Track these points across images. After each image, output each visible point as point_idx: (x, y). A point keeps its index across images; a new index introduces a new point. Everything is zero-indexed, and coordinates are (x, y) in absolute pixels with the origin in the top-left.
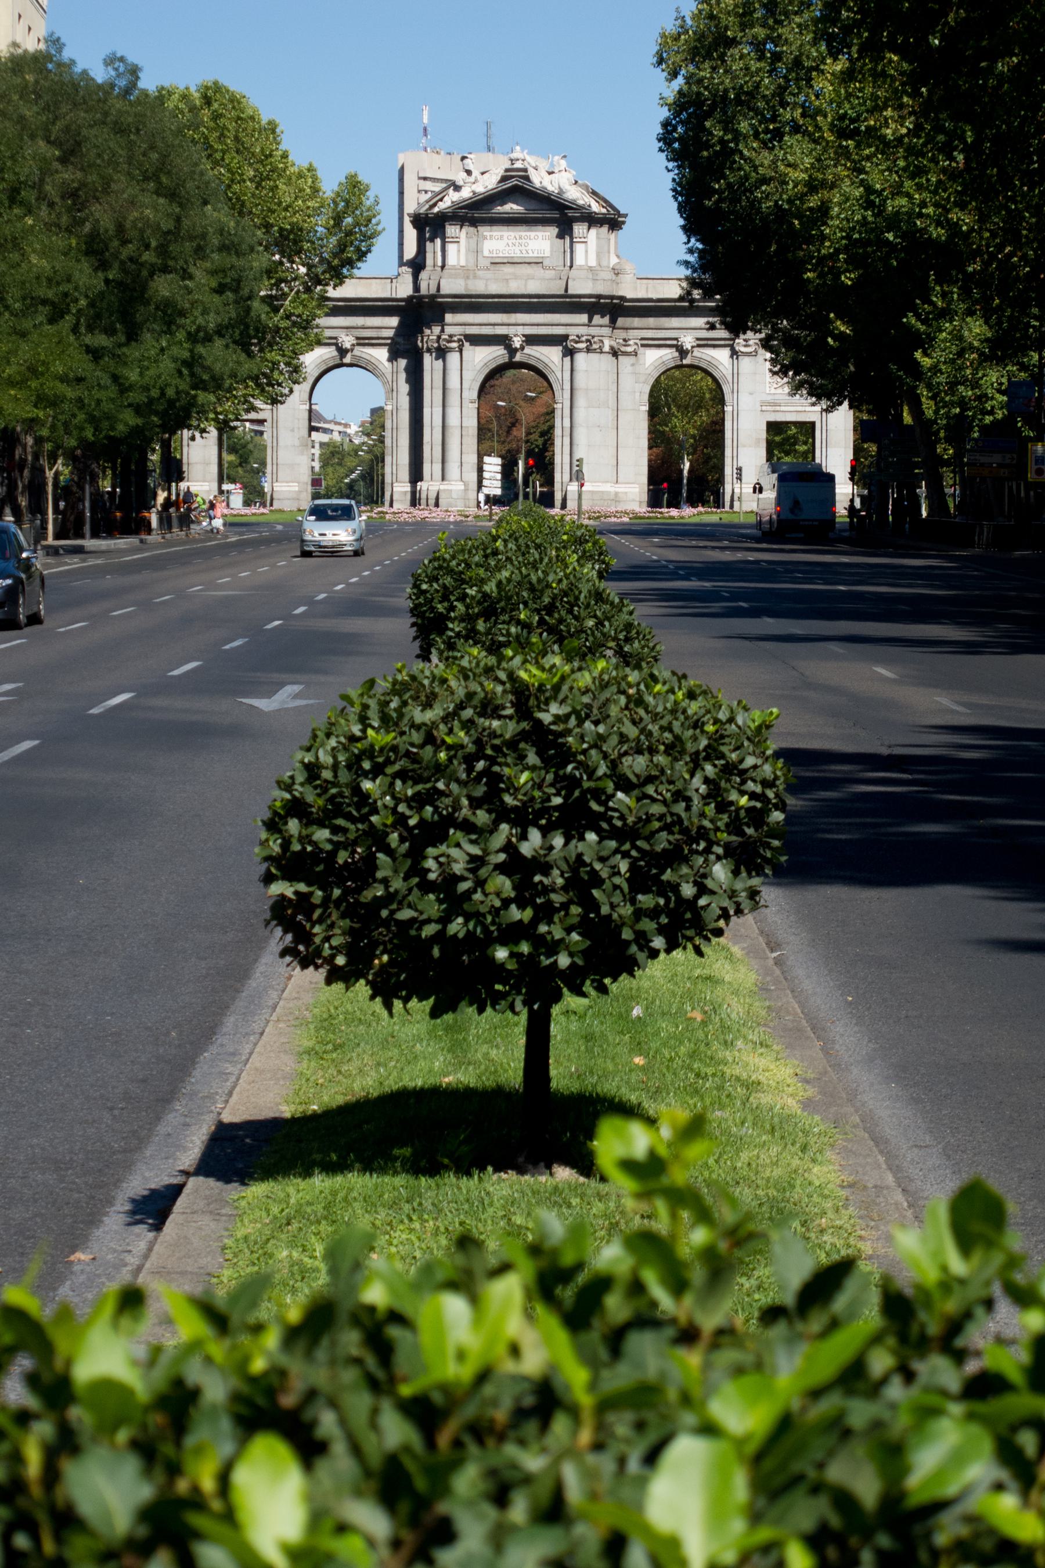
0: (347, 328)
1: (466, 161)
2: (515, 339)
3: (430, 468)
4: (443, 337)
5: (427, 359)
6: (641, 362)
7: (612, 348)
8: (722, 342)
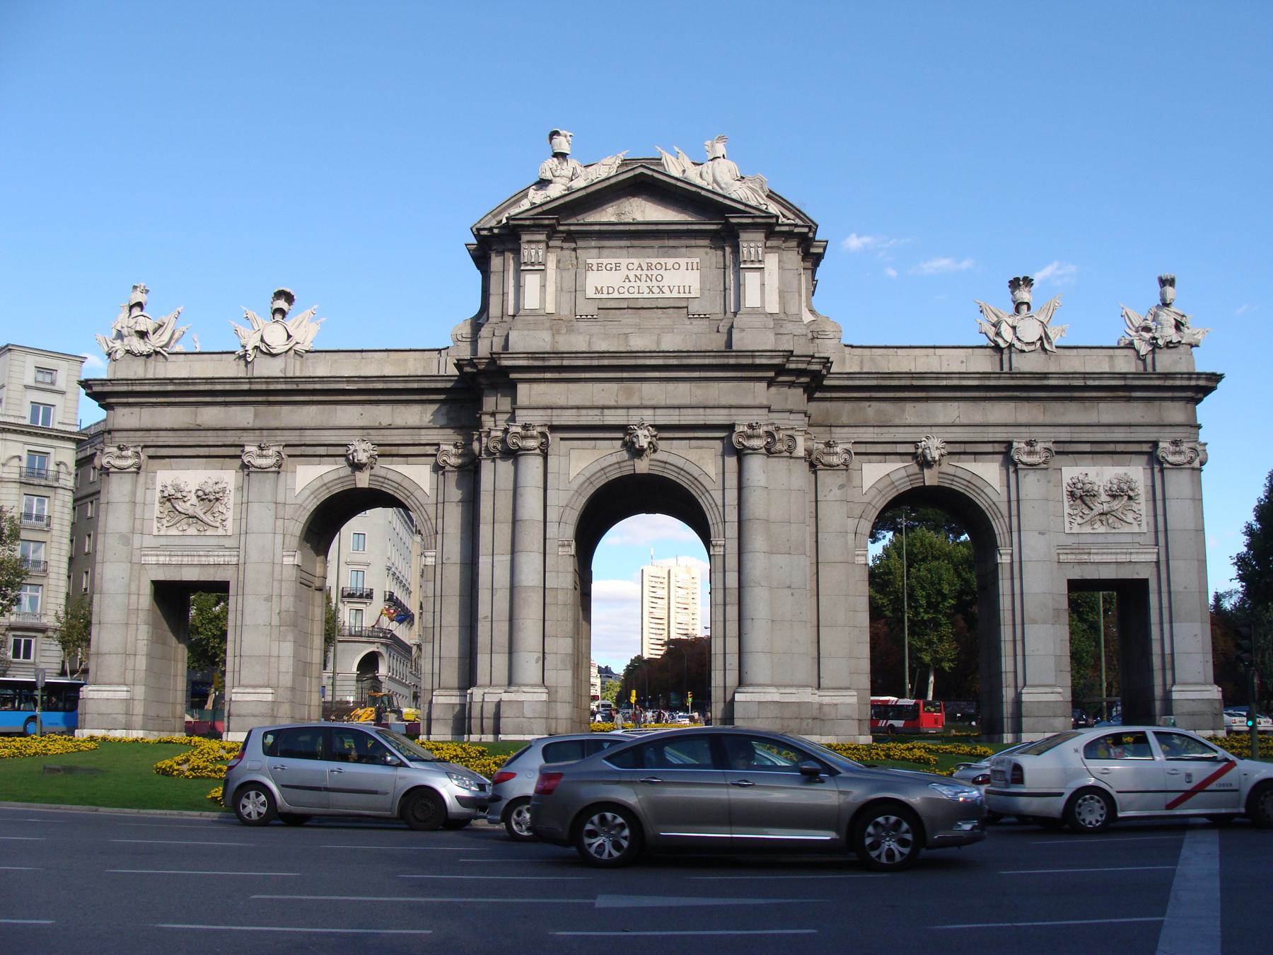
0: (362, 428)
1: (557, 140)
2: (639, 433)
3: (490, 664)
4: (513, 429)
5: (487, 468)
6: (856, 482)
7: (809, 452)
8: (988, 448)
